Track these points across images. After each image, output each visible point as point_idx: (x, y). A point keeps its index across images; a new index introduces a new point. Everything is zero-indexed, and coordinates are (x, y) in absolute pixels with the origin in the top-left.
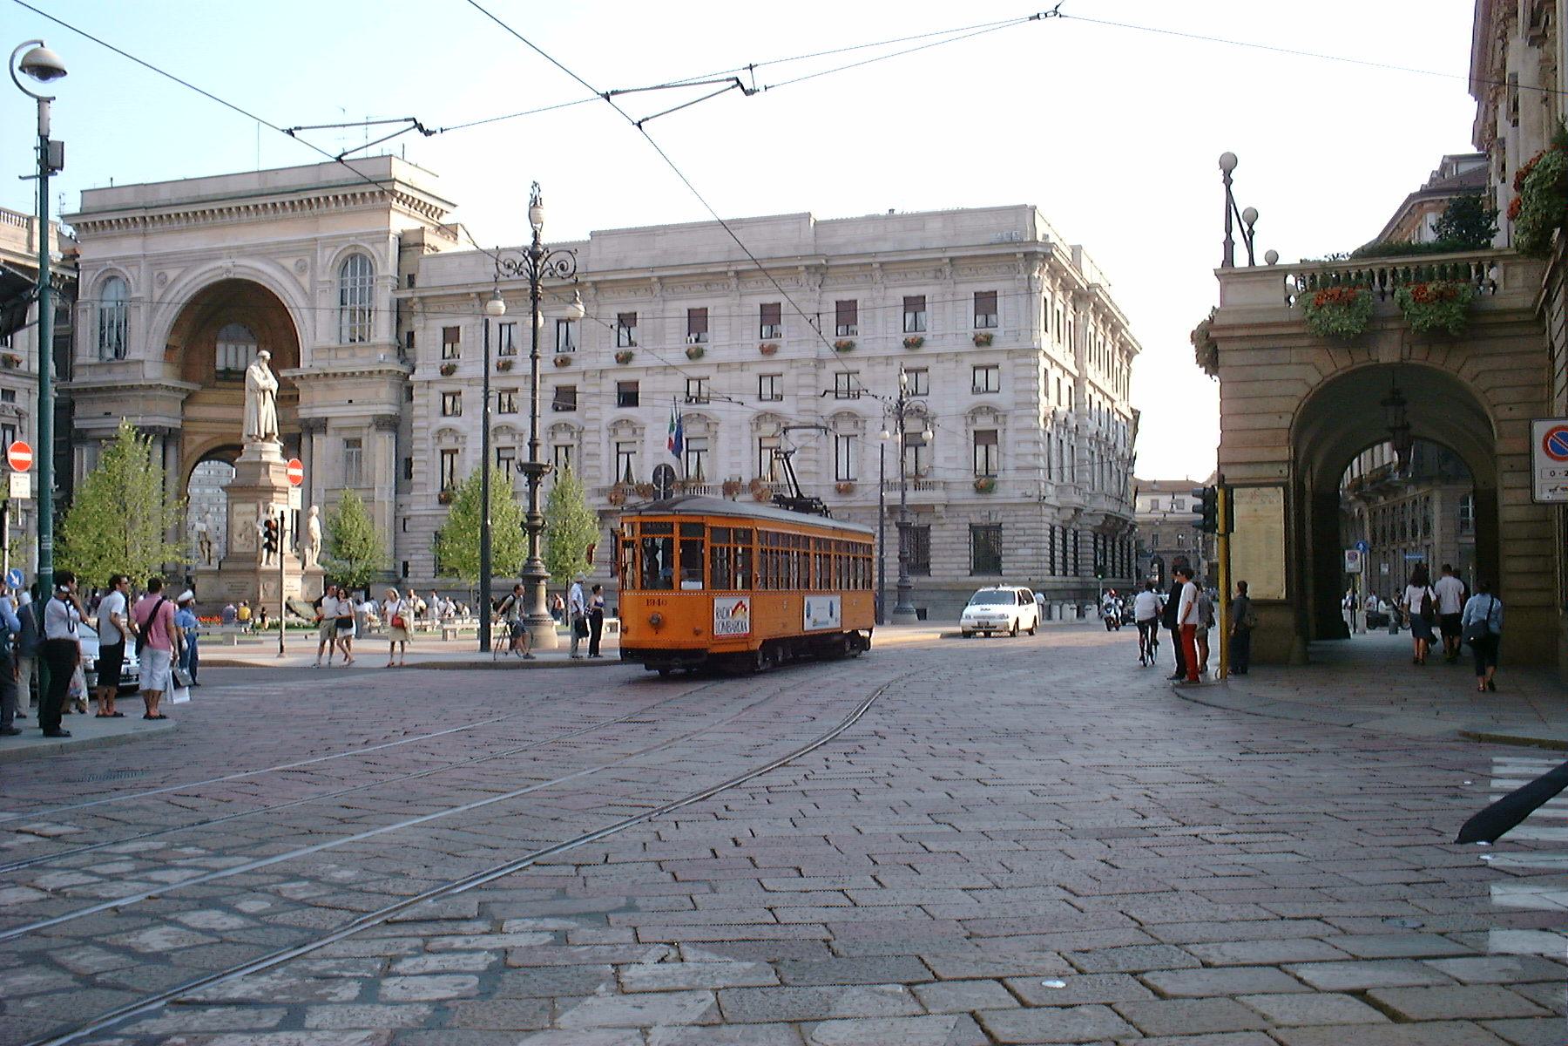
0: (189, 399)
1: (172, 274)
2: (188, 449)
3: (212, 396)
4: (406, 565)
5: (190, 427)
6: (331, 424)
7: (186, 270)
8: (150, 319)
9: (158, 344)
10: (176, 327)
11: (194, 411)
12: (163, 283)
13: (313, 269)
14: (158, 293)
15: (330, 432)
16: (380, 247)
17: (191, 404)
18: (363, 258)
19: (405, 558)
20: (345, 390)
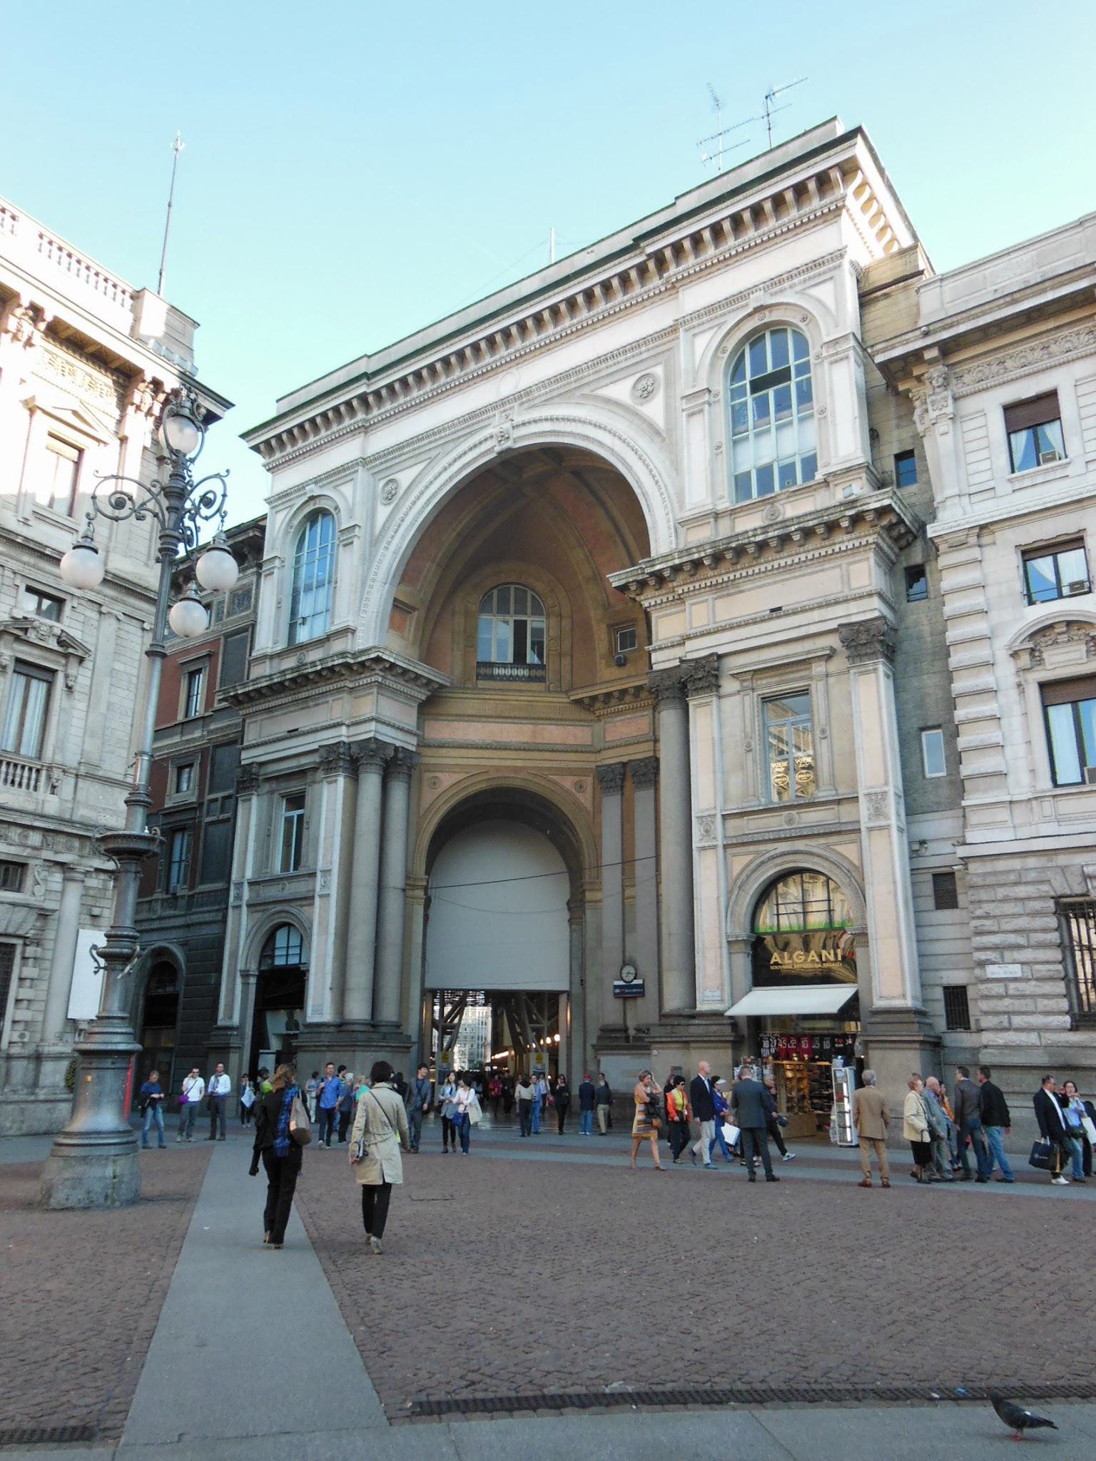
0: (432, 703)
1: (405, 478)
2: (428, 796)
3: (471, 705)
4: (956, 998)
5: (431, 757)
6: (733, 664)
7: (432, 460)
8: (368, 559)
9: (379, 596)
10: (409, 571)
11: (441, 731)
12: (389, 498)
13: (669, 383)
14: (383, 512)
15: (729, 685)
16: (824, 292)
17: (437, 717)
18: (778, 329)
19: (955, 977)
20: (754, 598)
